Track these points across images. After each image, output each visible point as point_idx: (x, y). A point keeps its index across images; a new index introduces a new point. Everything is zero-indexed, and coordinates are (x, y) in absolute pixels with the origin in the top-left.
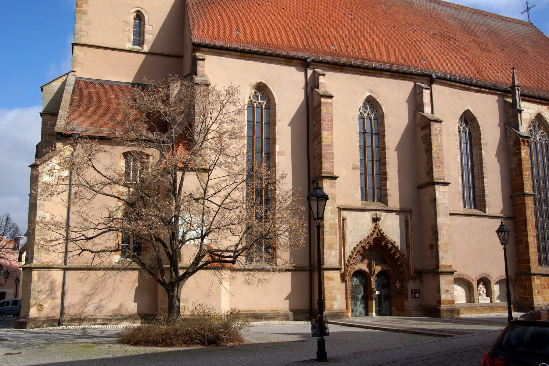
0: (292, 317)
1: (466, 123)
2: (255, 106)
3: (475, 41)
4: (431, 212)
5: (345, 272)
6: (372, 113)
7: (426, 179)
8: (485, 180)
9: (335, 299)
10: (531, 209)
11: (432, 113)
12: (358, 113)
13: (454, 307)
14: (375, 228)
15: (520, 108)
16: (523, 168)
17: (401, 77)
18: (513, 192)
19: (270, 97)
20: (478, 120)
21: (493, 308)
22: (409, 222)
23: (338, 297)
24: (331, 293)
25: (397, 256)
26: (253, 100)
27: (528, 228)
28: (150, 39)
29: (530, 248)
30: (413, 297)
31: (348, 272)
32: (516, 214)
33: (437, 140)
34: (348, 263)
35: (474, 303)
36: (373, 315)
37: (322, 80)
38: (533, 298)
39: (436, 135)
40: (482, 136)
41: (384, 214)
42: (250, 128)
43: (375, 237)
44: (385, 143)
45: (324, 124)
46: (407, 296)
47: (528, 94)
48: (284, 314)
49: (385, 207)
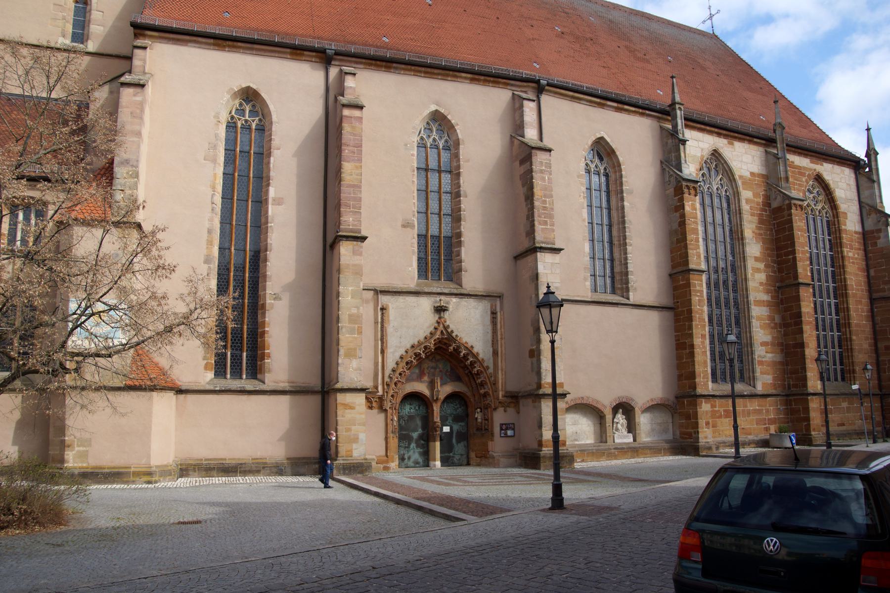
0: (289, 470)
1: (601, 159)
2: (239, 125)
3: (627, 47)
4: (531, 297)
5: (383, 395)
6: (441, 138)
7: (526, 244)
8: (629, 248)
9: (356, 440)
10: (699, 294)
11: (541, 139)
12: (416, 139)
13: (565, 451)
14: (438, 323)
15: (683, 136)
16: (687, 229)
17: (489, 81)
18: (673, 267)
19: (265, 112)
20: (618, 153)
21: (637, 451)
22: (499, 314)
23: (362, 436)
24: (348, 430)
25: (476, 370)
26: (235, 116)
27: (694, 323)
28: (98, 32)
29: (696, 355)
30: (502, 435)
31: (390, 395)
32: (678, 302)
33: (543, 179)
34: (389, 380)
35: (607, 442)
36: (435, 466)
37: (349, 82)
38: (698, 432)
39: (542, 172)
40: (624, 179)
41: (454, 300)
42: (229, 160)
43: (438, 338)
44: (459, 187)
45: (347, 151)
46: (493, 434)
47: (699, 119)
48: (275, 465)
49: (457, 289)
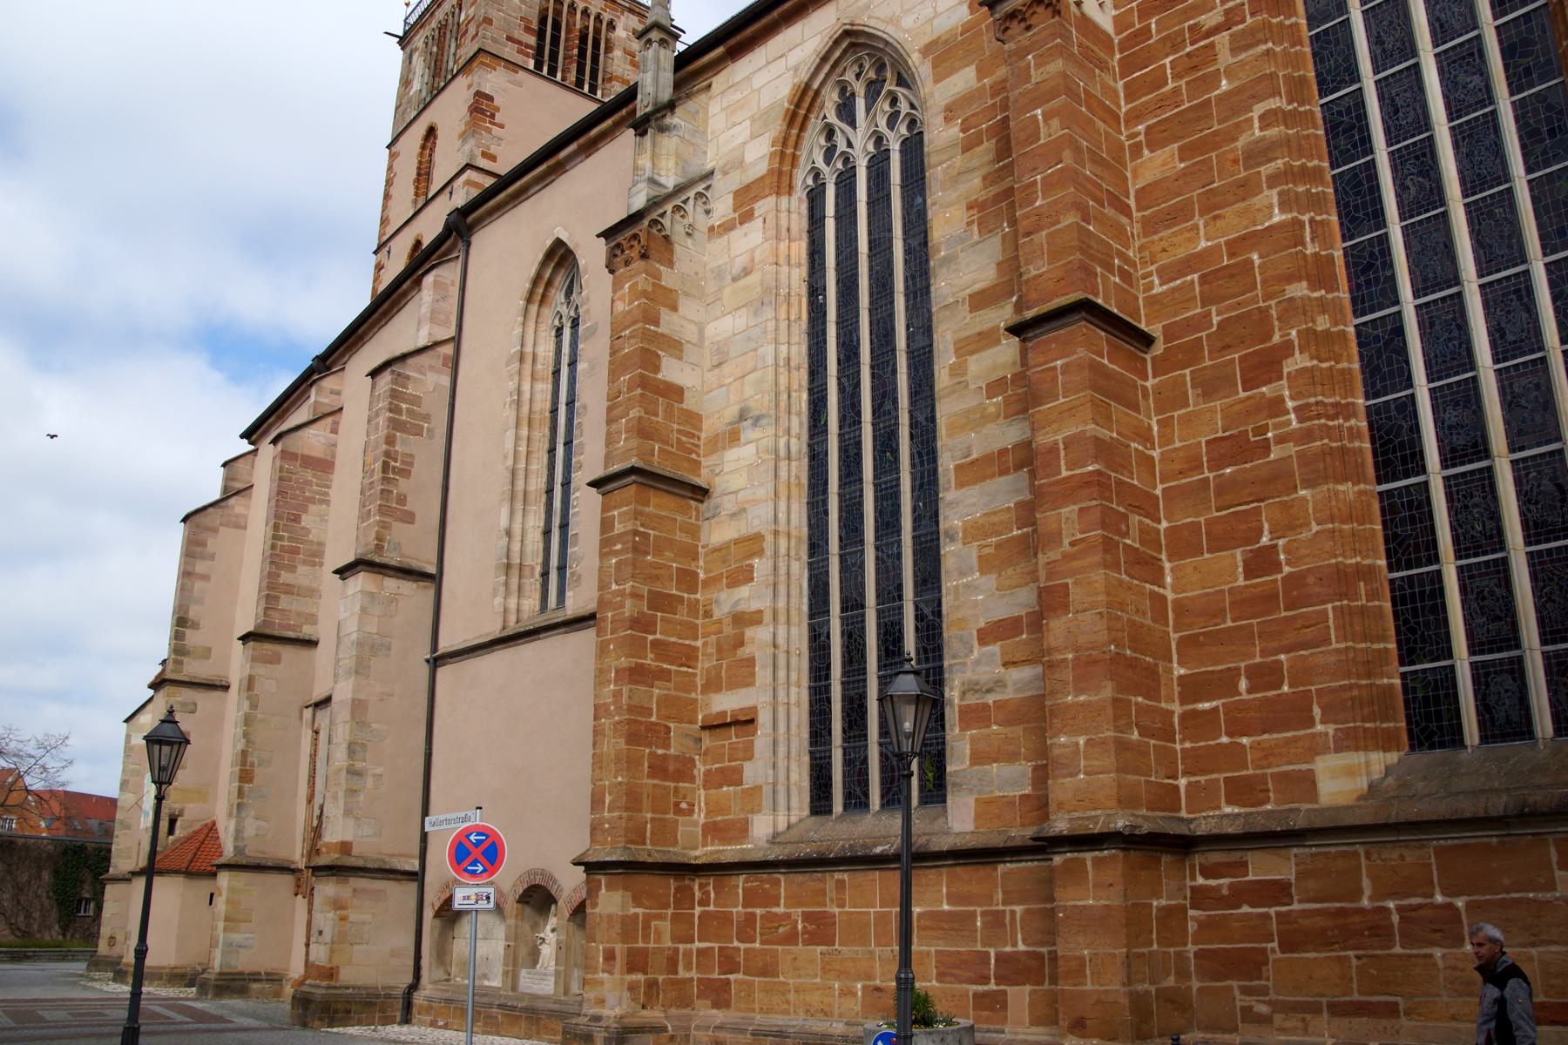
10: (619, 547)
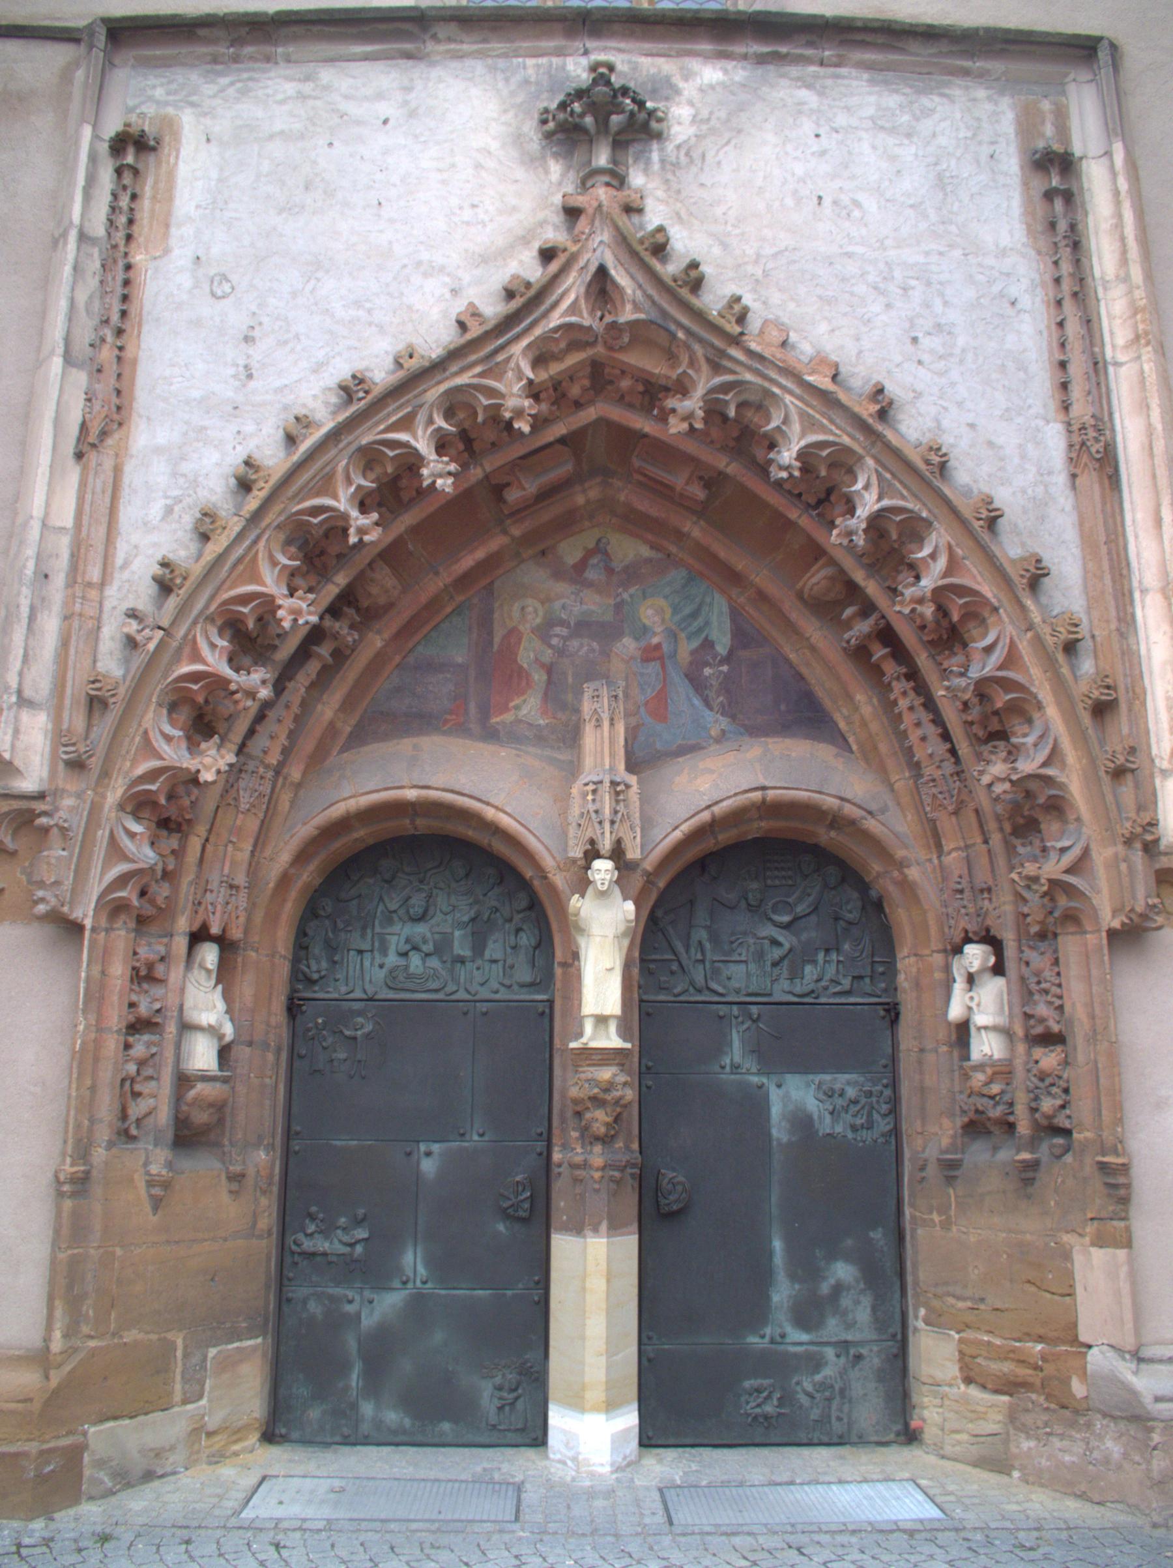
43: (574, 335)
